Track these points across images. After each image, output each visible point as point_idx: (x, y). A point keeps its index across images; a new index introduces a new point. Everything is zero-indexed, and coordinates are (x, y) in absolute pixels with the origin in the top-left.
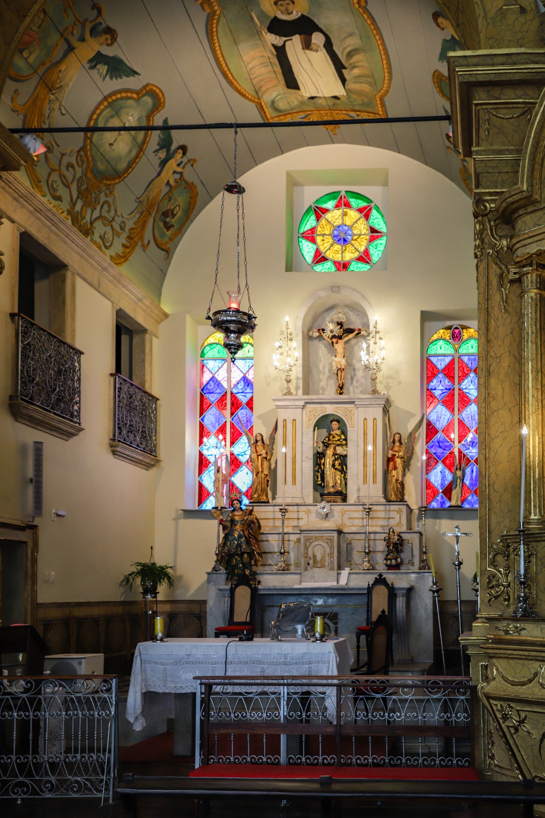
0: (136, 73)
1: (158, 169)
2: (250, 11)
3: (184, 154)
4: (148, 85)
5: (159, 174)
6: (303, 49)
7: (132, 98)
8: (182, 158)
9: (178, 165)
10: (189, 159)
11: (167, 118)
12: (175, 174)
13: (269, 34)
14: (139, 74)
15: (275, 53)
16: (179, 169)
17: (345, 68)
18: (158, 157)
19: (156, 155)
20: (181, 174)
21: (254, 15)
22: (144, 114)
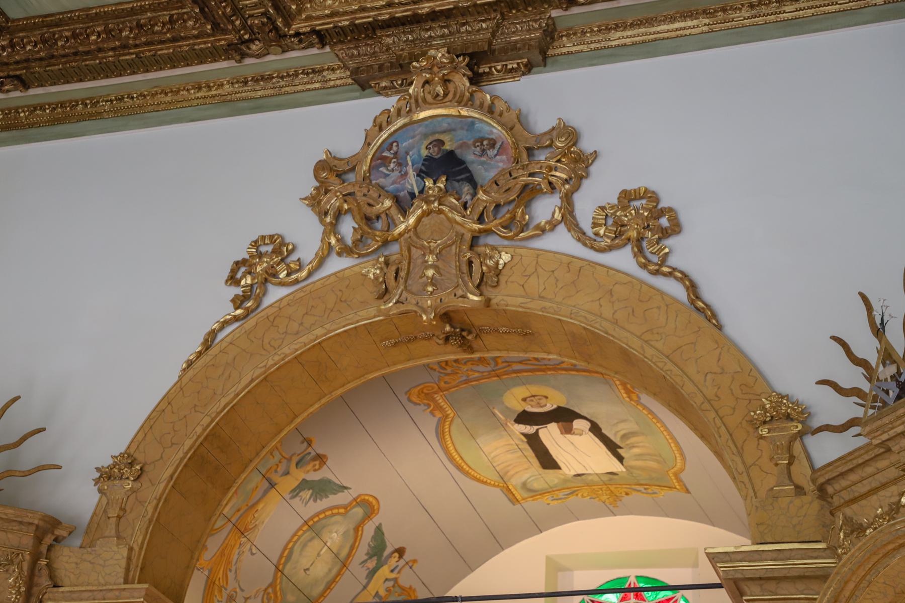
0: (346, 488)
1: (364, 582)
2: (491, 408)
3: (401, 557)
4: (359, 496)
5: (365, 587)
6: (562, 433)
7: (338, 514)
8: (397, 562)
9: (392, 571)
10: (407, 560)
11: (380, 524)
12: (387, 582)
13: (517, 425)
14: (350, 489)
15: (526, 440)
16: (393, 575)
17: (621, 448)
18: (366, 568)
19: (363, 567)
20: (395, 580)
21: (496, 412)
22: (352, 526)
